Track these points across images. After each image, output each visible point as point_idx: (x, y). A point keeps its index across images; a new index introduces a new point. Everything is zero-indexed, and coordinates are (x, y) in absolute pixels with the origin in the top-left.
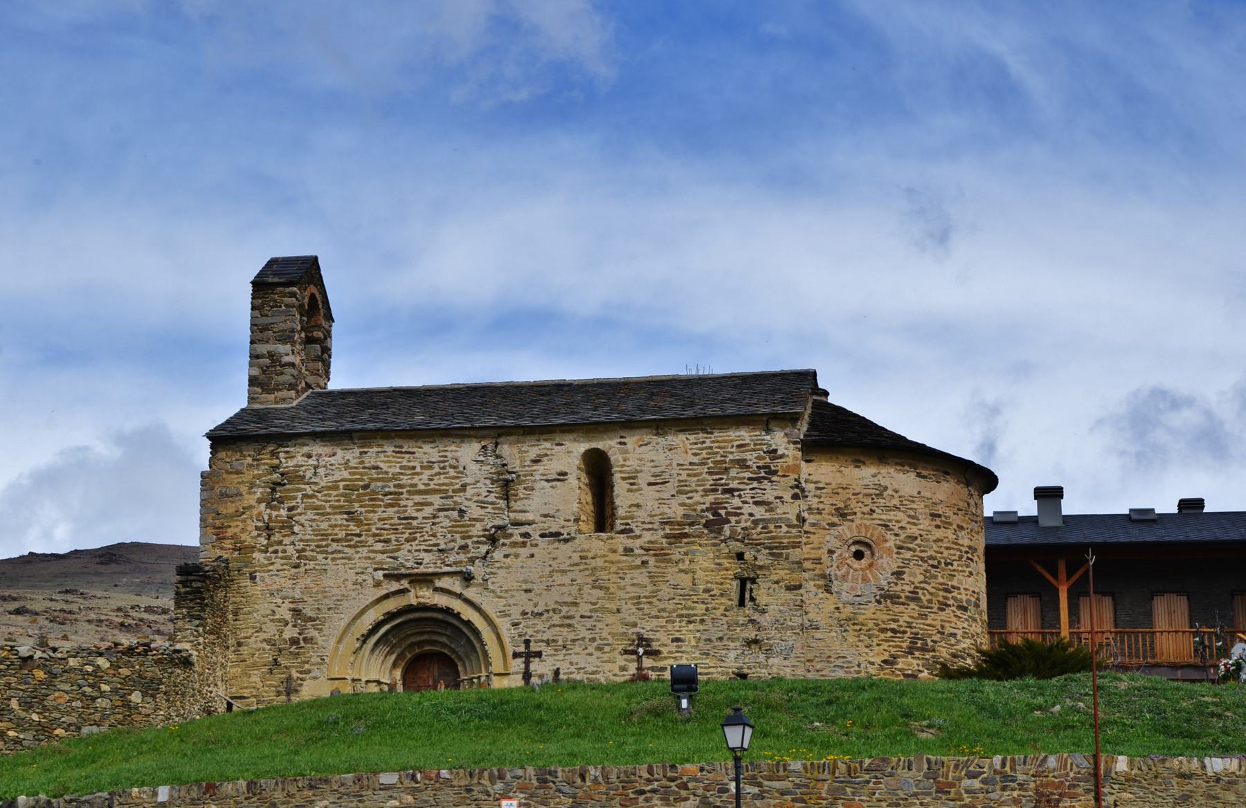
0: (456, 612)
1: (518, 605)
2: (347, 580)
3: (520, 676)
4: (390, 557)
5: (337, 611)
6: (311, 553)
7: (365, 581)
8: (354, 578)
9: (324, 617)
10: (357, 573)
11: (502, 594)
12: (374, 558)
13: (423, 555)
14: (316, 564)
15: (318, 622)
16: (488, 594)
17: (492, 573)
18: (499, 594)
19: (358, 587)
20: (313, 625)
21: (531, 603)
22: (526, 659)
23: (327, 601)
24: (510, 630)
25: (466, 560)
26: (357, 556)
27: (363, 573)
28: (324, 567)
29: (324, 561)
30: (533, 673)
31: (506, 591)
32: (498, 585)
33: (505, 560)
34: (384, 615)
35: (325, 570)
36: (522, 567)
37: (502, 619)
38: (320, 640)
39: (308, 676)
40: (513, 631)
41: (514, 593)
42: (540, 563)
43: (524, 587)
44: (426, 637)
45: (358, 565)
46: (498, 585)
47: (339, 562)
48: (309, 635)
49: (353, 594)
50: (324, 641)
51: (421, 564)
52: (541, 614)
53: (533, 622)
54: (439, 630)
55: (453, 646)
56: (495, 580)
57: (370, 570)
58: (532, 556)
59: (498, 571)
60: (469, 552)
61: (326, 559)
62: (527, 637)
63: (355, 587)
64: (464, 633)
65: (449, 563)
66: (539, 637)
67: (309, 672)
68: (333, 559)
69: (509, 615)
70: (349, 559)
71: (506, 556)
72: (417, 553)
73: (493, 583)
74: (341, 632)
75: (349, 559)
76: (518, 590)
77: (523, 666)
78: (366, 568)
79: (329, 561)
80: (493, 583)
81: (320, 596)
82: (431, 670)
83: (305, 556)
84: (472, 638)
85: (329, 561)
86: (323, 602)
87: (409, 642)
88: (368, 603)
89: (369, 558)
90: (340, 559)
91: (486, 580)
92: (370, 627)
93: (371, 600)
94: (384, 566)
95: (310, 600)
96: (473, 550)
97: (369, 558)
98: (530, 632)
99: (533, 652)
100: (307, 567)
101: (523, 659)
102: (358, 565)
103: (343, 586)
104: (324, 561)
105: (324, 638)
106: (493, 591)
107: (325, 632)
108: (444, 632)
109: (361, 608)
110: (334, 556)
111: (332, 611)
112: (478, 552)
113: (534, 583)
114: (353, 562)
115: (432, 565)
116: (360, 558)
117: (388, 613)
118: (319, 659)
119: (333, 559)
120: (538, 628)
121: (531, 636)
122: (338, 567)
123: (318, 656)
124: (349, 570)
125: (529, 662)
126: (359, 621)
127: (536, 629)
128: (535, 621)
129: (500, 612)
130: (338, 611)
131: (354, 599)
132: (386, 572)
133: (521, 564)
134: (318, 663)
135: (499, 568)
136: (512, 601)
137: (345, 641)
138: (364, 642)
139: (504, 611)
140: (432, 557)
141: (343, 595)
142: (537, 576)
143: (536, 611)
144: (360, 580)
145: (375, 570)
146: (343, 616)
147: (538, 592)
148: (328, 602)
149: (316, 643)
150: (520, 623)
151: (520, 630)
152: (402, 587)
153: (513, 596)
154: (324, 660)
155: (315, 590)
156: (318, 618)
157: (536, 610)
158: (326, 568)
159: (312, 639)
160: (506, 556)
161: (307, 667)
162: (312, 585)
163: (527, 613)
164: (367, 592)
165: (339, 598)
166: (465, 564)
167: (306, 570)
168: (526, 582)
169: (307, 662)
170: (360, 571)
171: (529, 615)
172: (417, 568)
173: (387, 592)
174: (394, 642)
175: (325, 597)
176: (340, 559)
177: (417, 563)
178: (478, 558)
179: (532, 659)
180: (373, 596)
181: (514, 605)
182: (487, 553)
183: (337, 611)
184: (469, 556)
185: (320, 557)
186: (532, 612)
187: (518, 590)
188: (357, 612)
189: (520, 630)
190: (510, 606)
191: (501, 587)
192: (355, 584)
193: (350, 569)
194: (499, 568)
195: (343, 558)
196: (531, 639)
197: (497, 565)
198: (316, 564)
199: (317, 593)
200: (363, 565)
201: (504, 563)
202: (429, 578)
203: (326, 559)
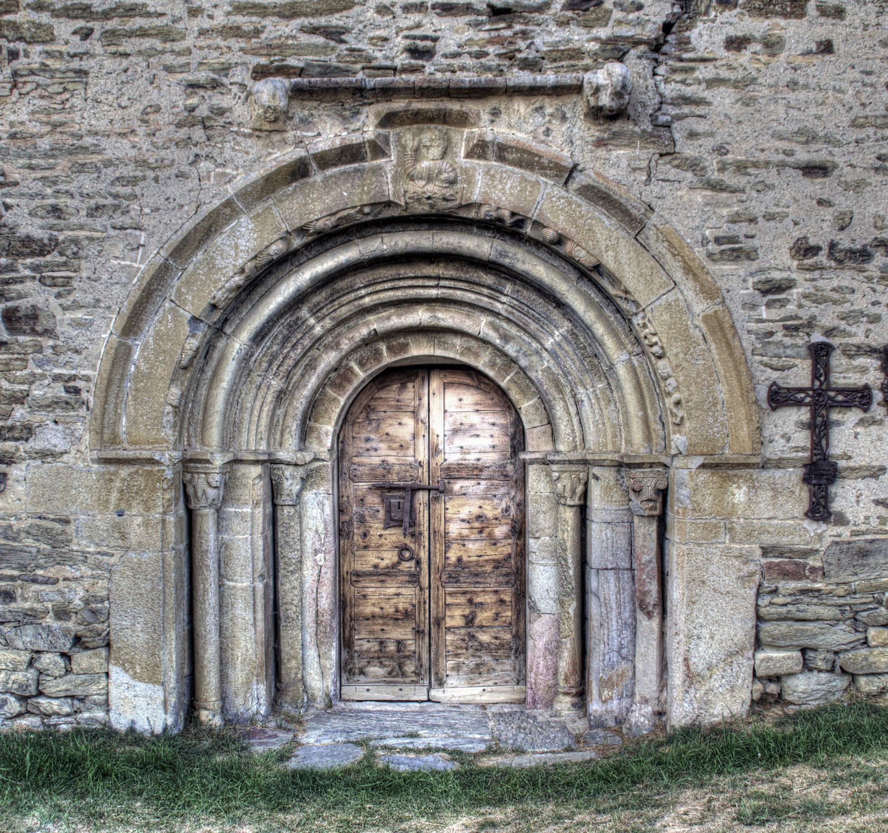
0: (549, 234)
1: (783, 216)
2: (158, 109)
3: (792, 476)
4: (314, 30)
5: (119, 220)
6: (34, 16)
7: (221, 112)
8: (182, 101)
9: (76, 241)
10: (193, 86)
11: (730, 178)
12: (257, 32)
13: (432, 23)
14: (49, 54)
15: (53, 257)
16: (673, 174)
17: (687, 100)
18: (715, 176)
19: (198, 134)
20: (35, 268)
21: (828, 214)
22: (814, 415)
23: (86, 182)
24: (754, 307)
25: (593, 46)
26: (196, 24)
27: (215, 85)
28: (76, 64)
29: (77, 44)
30: (842, 464)
31: (741, 168)
32: (709, 143)
33: (730, 56)
34: (286, 238)
35: (82, 73)
36: (793, 85)
37: (728, 267)
38: (63, 322)
39: (22, 446)
40: (764, 313)
41: (771, 176)
42: (855, 74)
43: (802, 155)
44: (420, 316)
45: (197, 56)
46: (709, 143)
47: (127, 46)
48: (24, 304)
49: (181, 156)
50: (78, 324)
51: (427, 54)
52: (863, 255)
53: (835, 283)
54: (470, 297)
55: (511, 349)
56: (701, 127)
57: (240, 75)
58: (827, 47)
59: (707, 94)
60: (603, 20)
61: (86, 34)
62: (817, 337)
63: (183, 133)
64: (560, 304)
65: (532, 55)
66: (858, 335)
67: (28, 431)
68: (111, 36)
69: (750, 255)
70: (166, 35)
71: (736, 44)
72: (414, 18)
73: (693, 135)
74: (136, 295)
75: (166, 35)
76: (781, 166)
77: (802, 438)
78: (225, 69)
79: (95, 45)
80: (693, 135)
81: (63, 163)
82: (423, 414)
83: (15, 26)
84: (599, 329)
85: (95, 45)
86: (72, 187)
87: (364, 331)
88: (230, 190)
89: (235, 31)
90: (131, 34)
91: (667, 126)
92: (238, 280)
93: (242, 180)
94: (292, 61)
95: (30, 182)
96: (617, 14)
97: (235, 31)
98: (828, 317)
99: (840, 391)
100: (18, 64)
101: (804, 414)
102: (197, 56)
103: (141, 131)
104: (77, 44)
105: (79, 315)
106: (694, 165)
107: (77, 295)
108: (485, 301)
109: (205, 210)
110: (112, 24)
111: (102, 221)
112: (639, 23)
113: (838, 144)
114: (179, 46)
115: (467, 61)
116: (202, 33)
117: (302, 231)
118: (58, 391)
119: (111, 36)
120: (860, 303)
121: (830, 332)
122: (125, 63)
123: (57, 378)
124: (162, 74)
125: (827, 425)
126: (200, 255)
127: (847, 307)
128: (845, 278)
129: (718, 240)
130: (127, 220)
131: (181, 175)
132: (295, 80)
133: (789, 75)
134: (55, 403)
135: (712, 83)
136: (758, 205)
137: (150, 330)
138: (219, 330)
139: (732, 240)
140: (470, 33)
141: (142, 163)
142: (845, 120)
143: (845, 244)
144: (203, 111)
145: (260, 73)
146: (143, 237)
147: (850, 176)
148: (88, 187)
149: (48, 333)
150: (789, 285)
151: (791, 308)
152: (356, 139)
153: (764, 187)
154: (77, 391)
155: (44, 144)
156: (52, 239)
157: (845, 243)
158: (85, 64)
159: (33, 315)
160: (736, 44)
161: (20, 413)
162: (34, 128)
163: (813, 250)
164: (228, 154)
165: (128, 171)
166: (588, 61)
167: (15, 74)
168: (809, 137)
169: (18, 399)
170: (202, 76)
171: (822, 258)
172: (413, 70)
173: (300, 153)
174: (318, 330)
175: (82, 168)
176: (131, 34)
177: (414, 52)
178: (637, 43)
179: (835, 416)
180: (249, 169)
181: (769, 217)
182: (667, 28)
183: (119, 220)
184: (603, 33)
185: (64, 28)
186: (832, 246)
187: (782, 165)
188: (189, 225)
189: (791, 308)
190: (752, 220)
191: (721, 150)
192: (190, 119)
193: (169, 69)
194: (712, 83)
195: (143, 33)
196: (835, 341)
197: (704, 72)
198: (49, 54)
199: (53, 152)
200: (214, 58)
201: (730, 67)
202: (454, 106)
203: (86, 34)
